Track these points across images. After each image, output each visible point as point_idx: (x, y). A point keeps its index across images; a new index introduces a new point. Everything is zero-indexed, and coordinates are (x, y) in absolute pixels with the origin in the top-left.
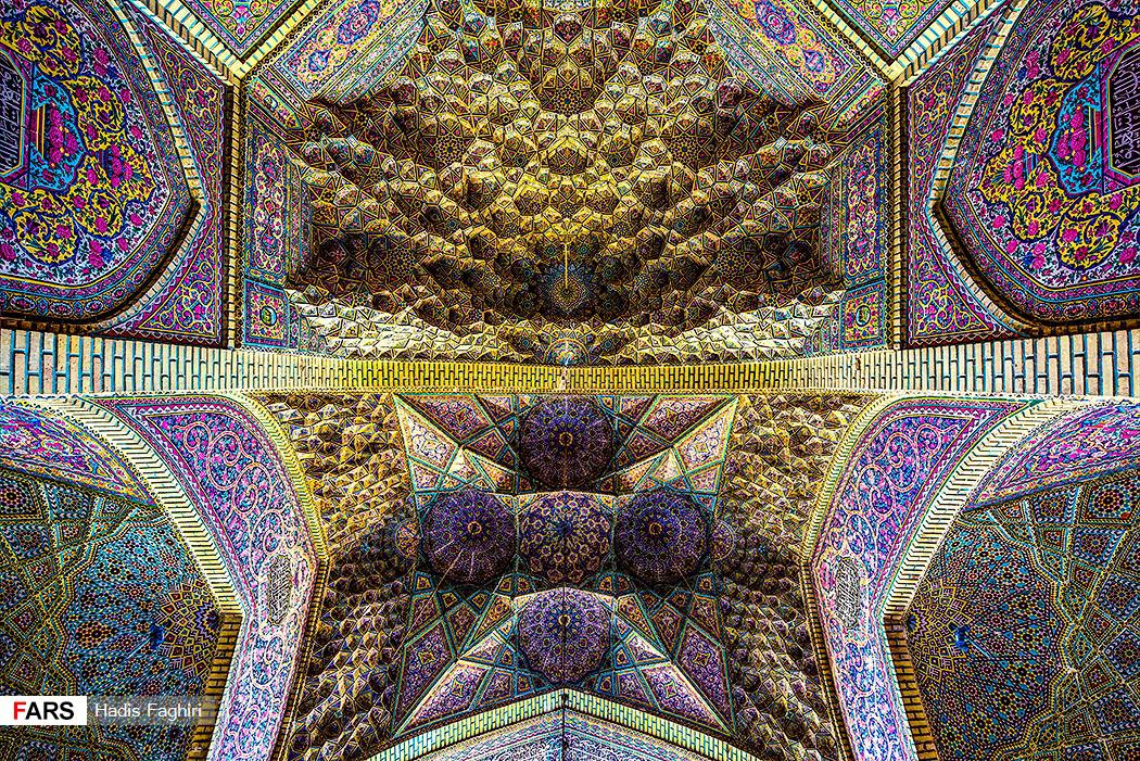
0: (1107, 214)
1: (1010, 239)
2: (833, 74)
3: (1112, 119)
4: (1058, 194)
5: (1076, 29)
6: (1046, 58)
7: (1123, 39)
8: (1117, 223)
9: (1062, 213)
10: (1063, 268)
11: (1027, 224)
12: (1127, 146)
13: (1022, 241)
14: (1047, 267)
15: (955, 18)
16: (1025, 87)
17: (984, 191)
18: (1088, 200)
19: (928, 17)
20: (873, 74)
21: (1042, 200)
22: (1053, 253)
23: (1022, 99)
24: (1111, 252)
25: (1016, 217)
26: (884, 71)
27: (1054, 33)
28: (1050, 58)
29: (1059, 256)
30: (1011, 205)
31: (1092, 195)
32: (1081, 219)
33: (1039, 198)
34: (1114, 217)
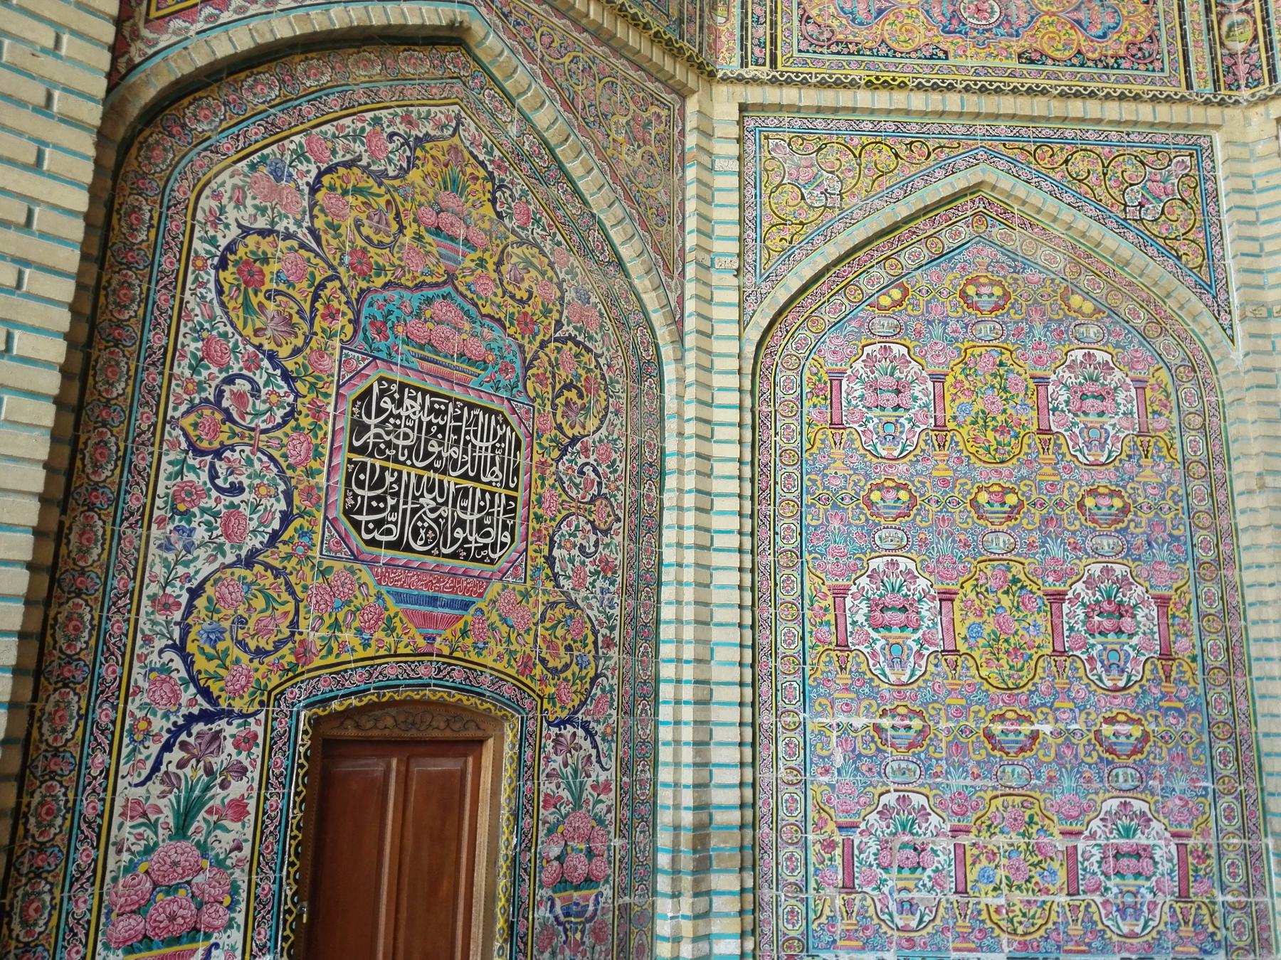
0: (307, 343)
1: (334, 152)
2: (814, 13)
3: (450, 398)
4: (378, 275)
5: (588, 390)
6: (580, 338)
7: (540, 444)
8: (284, 352)
9: (342, 270)
10: (235, 232)
11: (350, 198)
12: (400, 404)
13: (321, 174)
14: (249, 202)
15: (718, 246)
16: (563, 292)
17: (445, 144)
18: (342, 321)
19: (749, 214)
20: (752, 71)
21: (381, 245)
22: (273, 223)
23: (551, 280)
24: (234, 327)
25: (371, 181)
26: (739, 89)
27: (602, 361)
28: (577, 344)
29: (263, 233)
30: (397, 183)
31: (349, 329)
32: (316, 298)
33: (387, 240)
34: (296, 351)
